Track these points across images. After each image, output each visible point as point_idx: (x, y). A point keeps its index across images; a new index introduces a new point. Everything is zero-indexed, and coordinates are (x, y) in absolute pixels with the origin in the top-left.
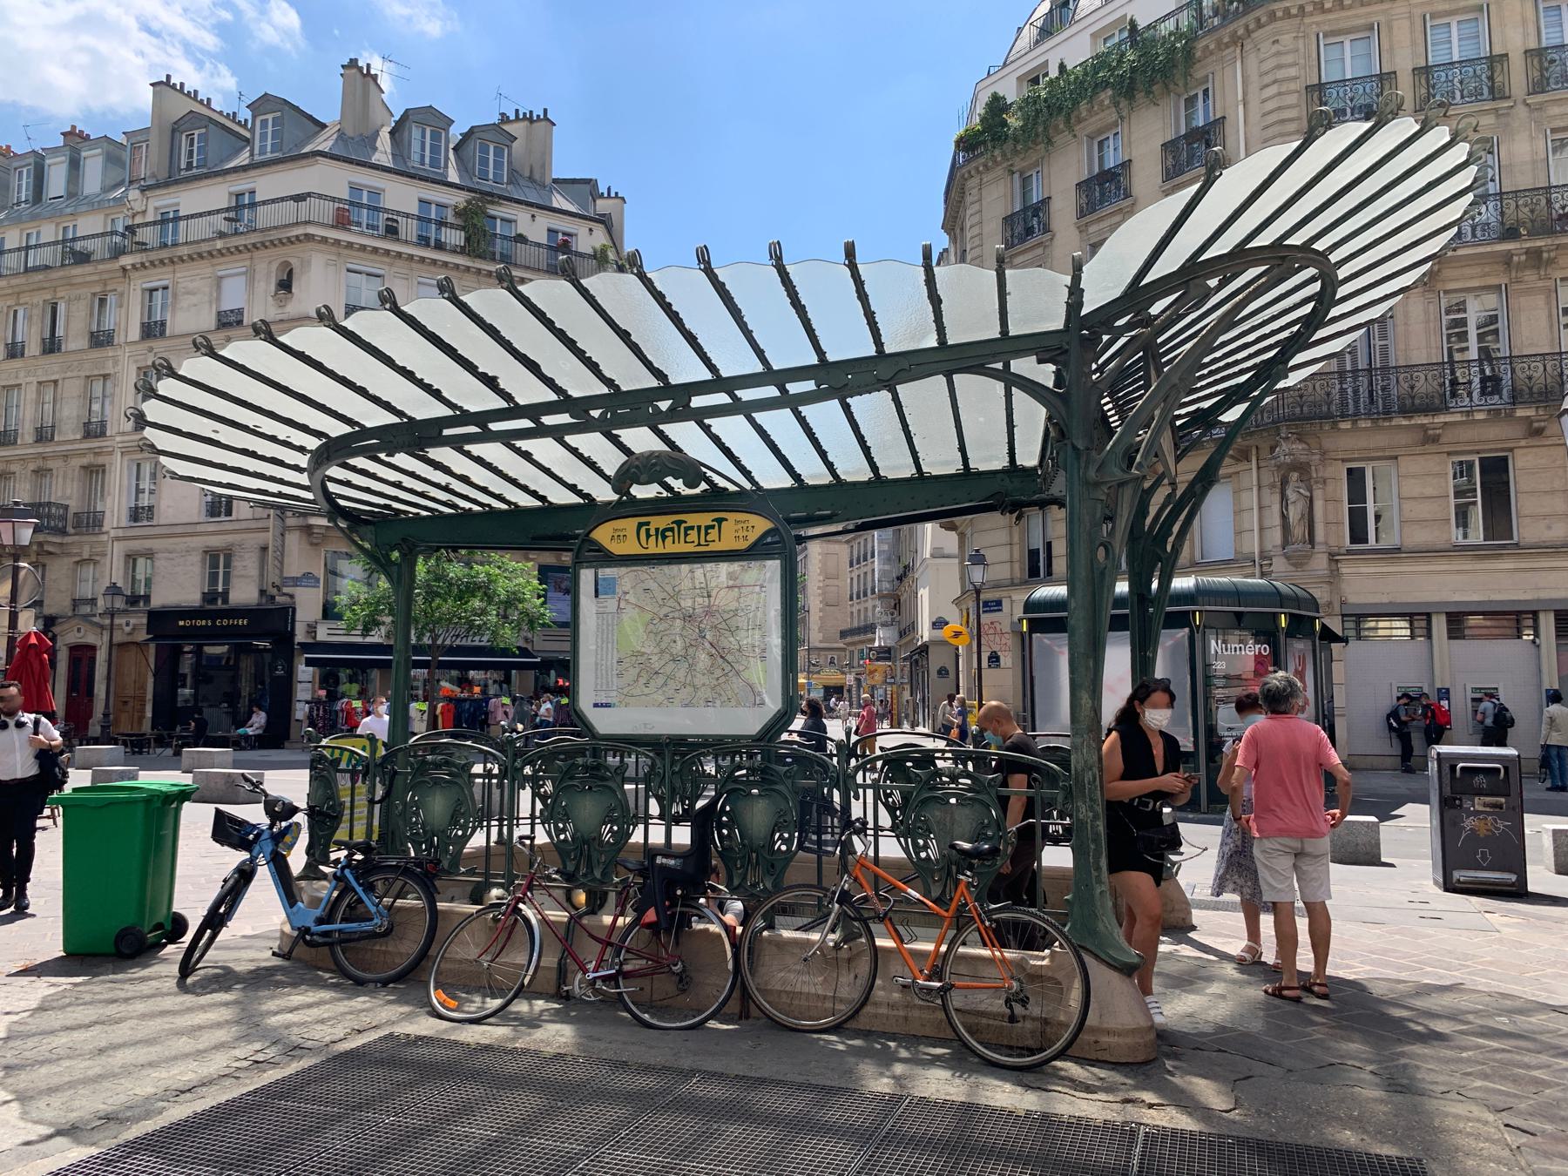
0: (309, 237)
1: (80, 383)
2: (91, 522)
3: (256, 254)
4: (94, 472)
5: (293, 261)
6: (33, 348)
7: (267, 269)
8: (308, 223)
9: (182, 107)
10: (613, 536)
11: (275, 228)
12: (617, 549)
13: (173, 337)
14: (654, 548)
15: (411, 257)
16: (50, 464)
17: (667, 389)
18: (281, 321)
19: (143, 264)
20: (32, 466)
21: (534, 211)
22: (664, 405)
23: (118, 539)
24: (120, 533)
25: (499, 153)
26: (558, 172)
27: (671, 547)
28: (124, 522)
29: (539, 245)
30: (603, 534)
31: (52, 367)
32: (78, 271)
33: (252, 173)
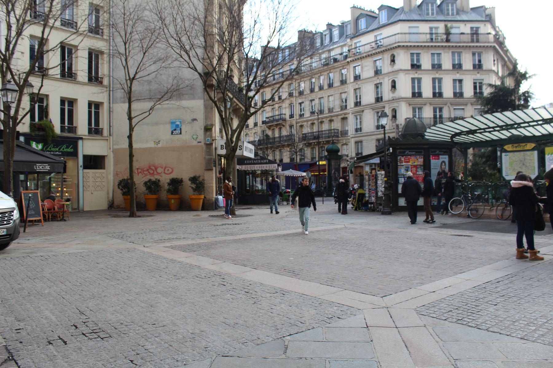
0: (399, 46)
1: (339, 95)
2: (345, 133)
3: (386, 53)
4: (344, 119)
5: (395, 54)
6: (326, 87)
7: (387, 57)
8: (399, 42)
9: (358, 13)
10: (508, 147)
11: (390, 45)
12: (508, 150)
13: (363, 80)
14: (515, 149)
15: (428, 46)
16: (333, 118)
17: (516, 124)
18: (393, 72)
19: (353, 60)
20: (328, 119)
21: (466, 23)
22: (516, 126)
23: (352, 137)
24: (353, 136)
25: (452, 6)
26: (472, 5)
27: (518, 149)
28: (354, 133)
29: (468, 34)
30: (506, 147)
31: (331, 91)
32: (336, 64)
33: (381, 29)
